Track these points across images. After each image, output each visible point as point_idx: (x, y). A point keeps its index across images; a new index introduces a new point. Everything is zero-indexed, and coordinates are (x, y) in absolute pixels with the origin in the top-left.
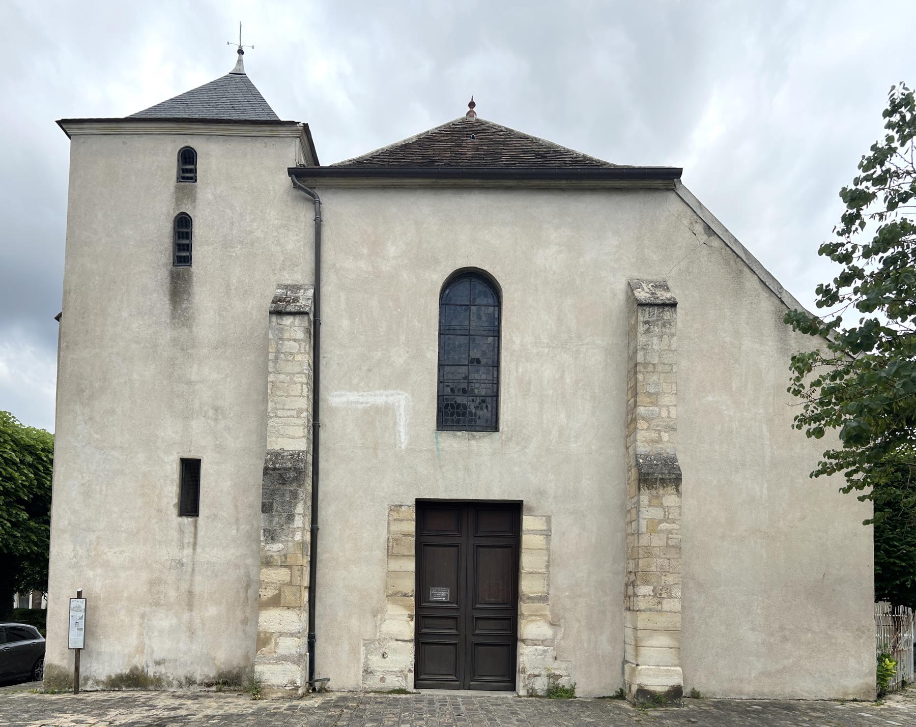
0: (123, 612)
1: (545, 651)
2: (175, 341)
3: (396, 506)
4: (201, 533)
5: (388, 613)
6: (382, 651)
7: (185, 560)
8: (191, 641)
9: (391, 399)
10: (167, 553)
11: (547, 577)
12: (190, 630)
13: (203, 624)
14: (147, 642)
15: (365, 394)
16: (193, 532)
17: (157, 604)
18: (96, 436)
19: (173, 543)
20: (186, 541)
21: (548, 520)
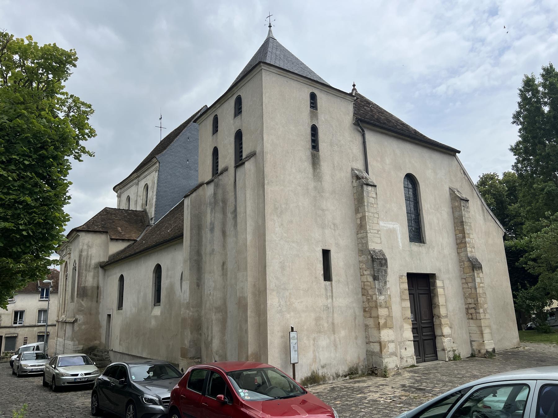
0: (305, 338)
1: (450, 340)
2: (315, 188)
3: (401, 276)
4: (334, 291)
5: (405, 327)
6: (405, 347)
7: (329, 305)
8: (336, 352)
9: (395, 226)
10: (322, 302)
11: (446, 306)
12: (335, 345)
13: (340, 341)
14: (317, 355)
15: (386, 223)
16: (331, 288)
17: (320, 332)
18: (284, 234)
19: (323, 296)
20: (328, 295)
21: (443, 283)
